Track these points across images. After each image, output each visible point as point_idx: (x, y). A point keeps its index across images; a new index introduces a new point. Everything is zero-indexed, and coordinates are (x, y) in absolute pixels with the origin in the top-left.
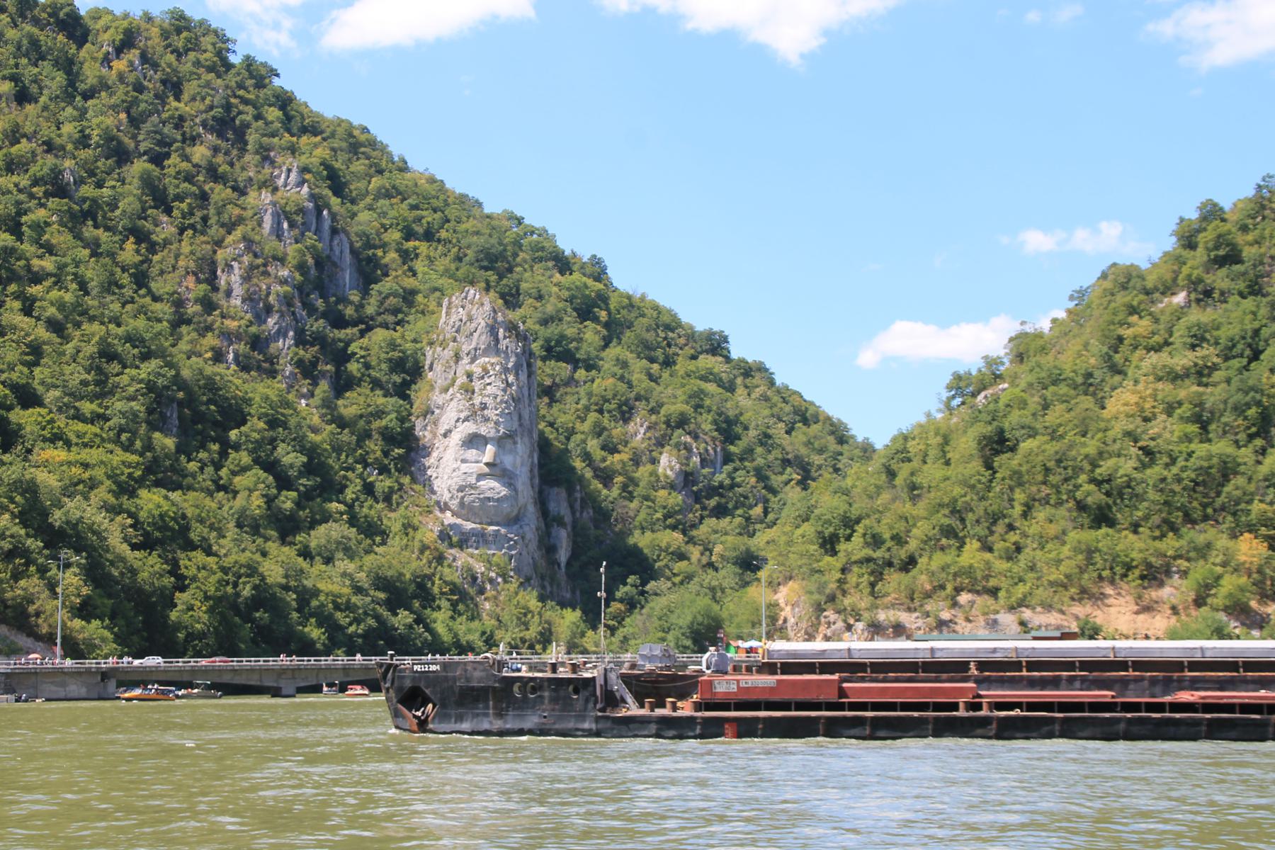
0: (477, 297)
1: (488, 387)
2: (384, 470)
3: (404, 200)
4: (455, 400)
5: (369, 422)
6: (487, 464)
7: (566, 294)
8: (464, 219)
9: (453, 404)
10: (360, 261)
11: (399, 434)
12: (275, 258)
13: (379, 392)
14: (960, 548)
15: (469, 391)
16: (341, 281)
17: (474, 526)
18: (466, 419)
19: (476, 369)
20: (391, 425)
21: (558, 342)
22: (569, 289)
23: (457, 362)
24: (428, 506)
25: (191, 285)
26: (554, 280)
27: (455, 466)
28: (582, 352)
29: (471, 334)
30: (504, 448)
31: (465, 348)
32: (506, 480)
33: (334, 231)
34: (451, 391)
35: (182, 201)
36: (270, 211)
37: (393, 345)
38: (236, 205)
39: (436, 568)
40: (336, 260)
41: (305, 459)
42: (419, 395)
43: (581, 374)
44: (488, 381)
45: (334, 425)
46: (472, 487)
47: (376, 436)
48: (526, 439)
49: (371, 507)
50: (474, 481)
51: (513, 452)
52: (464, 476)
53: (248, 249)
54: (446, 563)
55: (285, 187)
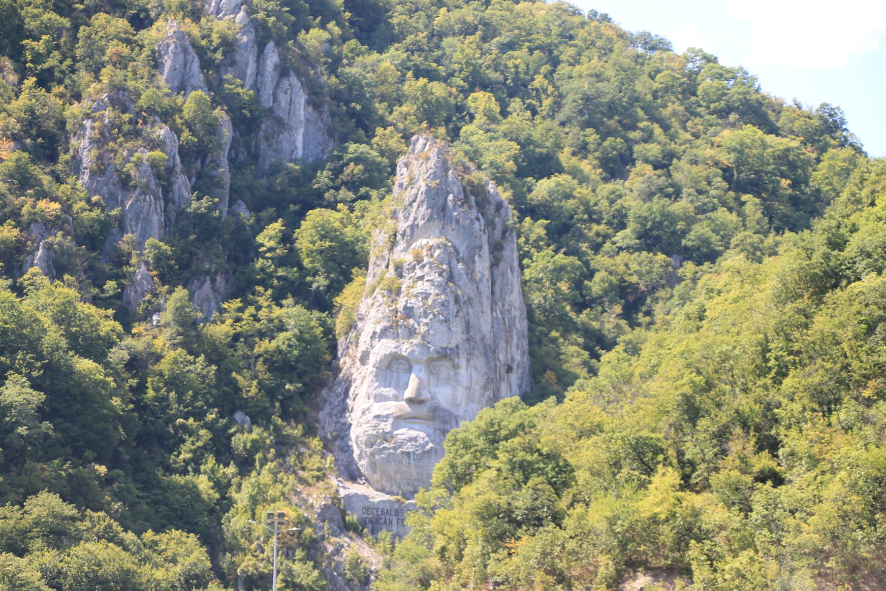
0: (427, 147)
1: (420, 283)
2: (259, 417)
3: (485, 39)
4: (377, 304)
5: (252, 348)
6: (410, 401)
7: (726, 159)
8: (584, 59)
9: (373, 312)
10: (333, 115)
11: (298, 360)
12: (151, 110)
13: (289, 301)
14: (643, 485)
15: (394, 292)
16: (286, 146)
17: (387, 497)
18: (384, 333)
19: (408, 258)
20: (284, 348)
21: (658, 225)
22: (730, 150)
23: (391, 249)
24: (319, 470)
25: (4, 155)
26: (717, 139)
27: (366, 406)
28: (692, 235)
29: (411, 204)
30: (437, 375)
31: (403, 225)
32: (438, 424)
33: (283, 72)
34: (375, 294)
35: (36, 39)
36: (172, 47)
37: (325, 233)
38: (128, 42)
39: (282, 563)
40: (281, 114)
41: (38, 397)
42: (346, 297)
43: (689, 267)
44: (419, 273)
45: (179, 350)
46: (386, 437)
47: (260, 366)
48: (479, 362)
49: (213, 471)
50: (388, 428)
51: (453, 380)
52: (375, 421)
53: (113, 101)
54: (299, 554)
55: (218, 13)
